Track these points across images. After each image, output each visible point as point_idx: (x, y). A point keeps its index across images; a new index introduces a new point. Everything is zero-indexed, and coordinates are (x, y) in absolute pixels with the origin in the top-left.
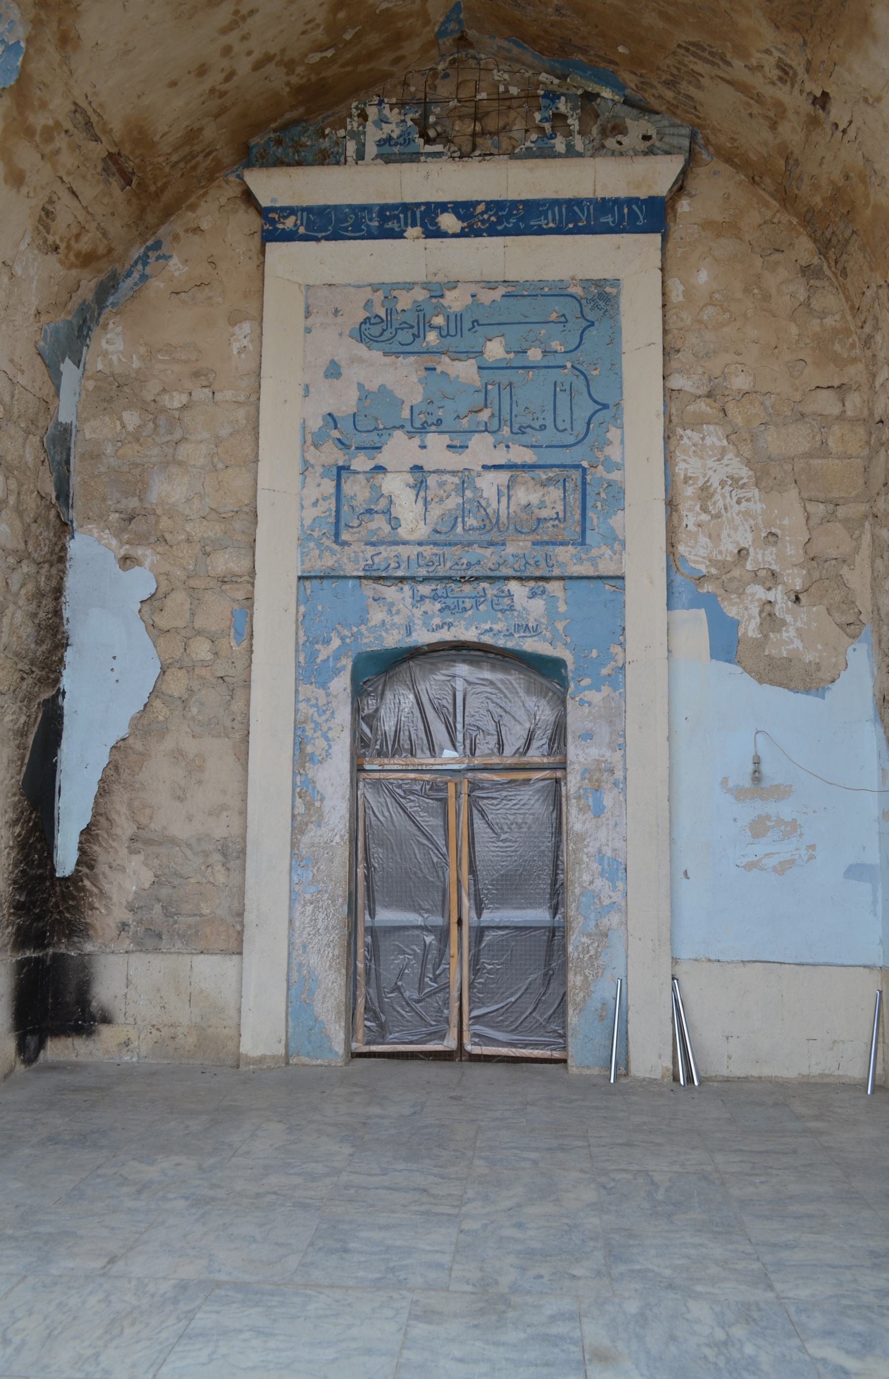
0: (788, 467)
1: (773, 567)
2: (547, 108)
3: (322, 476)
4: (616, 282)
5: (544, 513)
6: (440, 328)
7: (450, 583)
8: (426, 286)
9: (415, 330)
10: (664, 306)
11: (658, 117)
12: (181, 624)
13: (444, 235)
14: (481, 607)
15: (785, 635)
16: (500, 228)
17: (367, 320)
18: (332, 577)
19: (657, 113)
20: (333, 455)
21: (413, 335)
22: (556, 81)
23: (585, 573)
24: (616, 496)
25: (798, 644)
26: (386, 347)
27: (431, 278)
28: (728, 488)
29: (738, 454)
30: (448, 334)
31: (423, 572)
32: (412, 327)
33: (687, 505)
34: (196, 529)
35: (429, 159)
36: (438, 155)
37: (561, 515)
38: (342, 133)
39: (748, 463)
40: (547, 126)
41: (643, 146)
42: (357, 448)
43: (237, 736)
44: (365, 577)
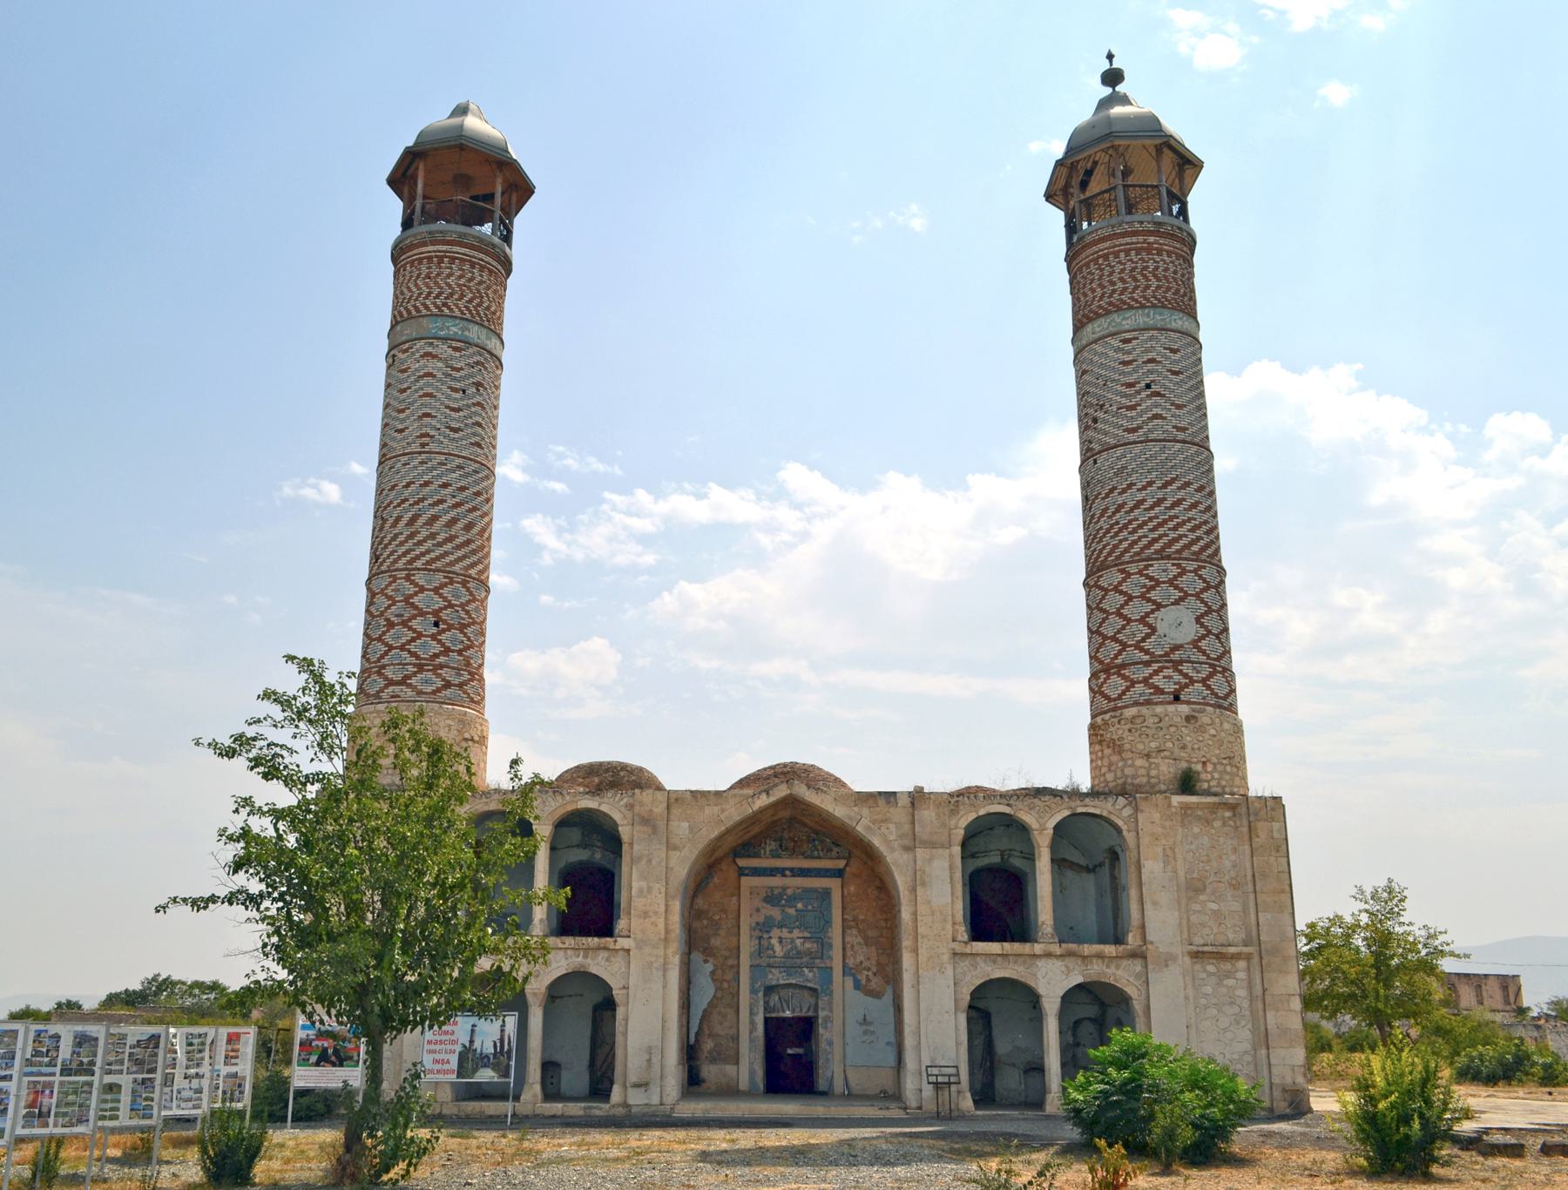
7: (788, 969)
20: (758, 933)
24: (831, 946)
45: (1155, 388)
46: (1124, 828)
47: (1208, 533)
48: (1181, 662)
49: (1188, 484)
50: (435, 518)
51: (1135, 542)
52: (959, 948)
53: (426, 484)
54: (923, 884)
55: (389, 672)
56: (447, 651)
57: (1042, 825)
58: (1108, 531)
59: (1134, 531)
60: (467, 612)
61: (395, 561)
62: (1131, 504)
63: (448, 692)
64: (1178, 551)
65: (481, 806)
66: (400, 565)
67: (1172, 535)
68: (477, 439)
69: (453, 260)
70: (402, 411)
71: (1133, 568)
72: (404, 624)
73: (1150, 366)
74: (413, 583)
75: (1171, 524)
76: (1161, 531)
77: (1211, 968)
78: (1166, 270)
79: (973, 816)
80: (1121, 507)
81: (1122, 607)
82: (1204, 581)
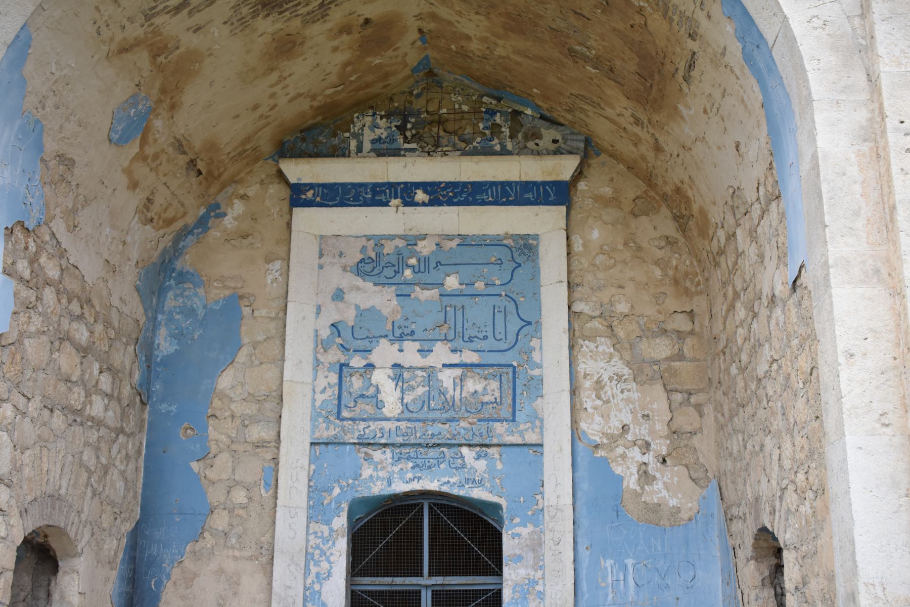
0: (656, 367)
1: (647, 438)
2: (488, 120)
3: (329, 370)
4: (536, 237)
5: (486, 399)
6: (413, 266)
8: (403, 237)
9: (396, 268)
10: (568, 254)
11: (563, 128)
12: (224, 476)
13: (417, 204)
14: (442, 466)
15: (655, 487)
16: (455, 200)
17: (362, 261)
18: (335, 443)
19: (562, 125)
20: (335, 356)
21: (395, 271)
22: (494, 102)
23: (515, 442)
24: (536, 385)
25: (665, 493)
26: (376, 279)
27: (407, 232)
28: (614, 382)
29: (621, 358)
30: (419, 271)
31: (400, 440)
32: (394, 266)
33: (586, 394)
34: (238, 408)
35: (407, 153)
36: (413, 150)
37: (498, 400)
38: (347, 135)
39: (628, 364)
40: (487, 132)
41: (553, 147)
42: (354, 351)
43: (264, 560)
44: (358, 444)
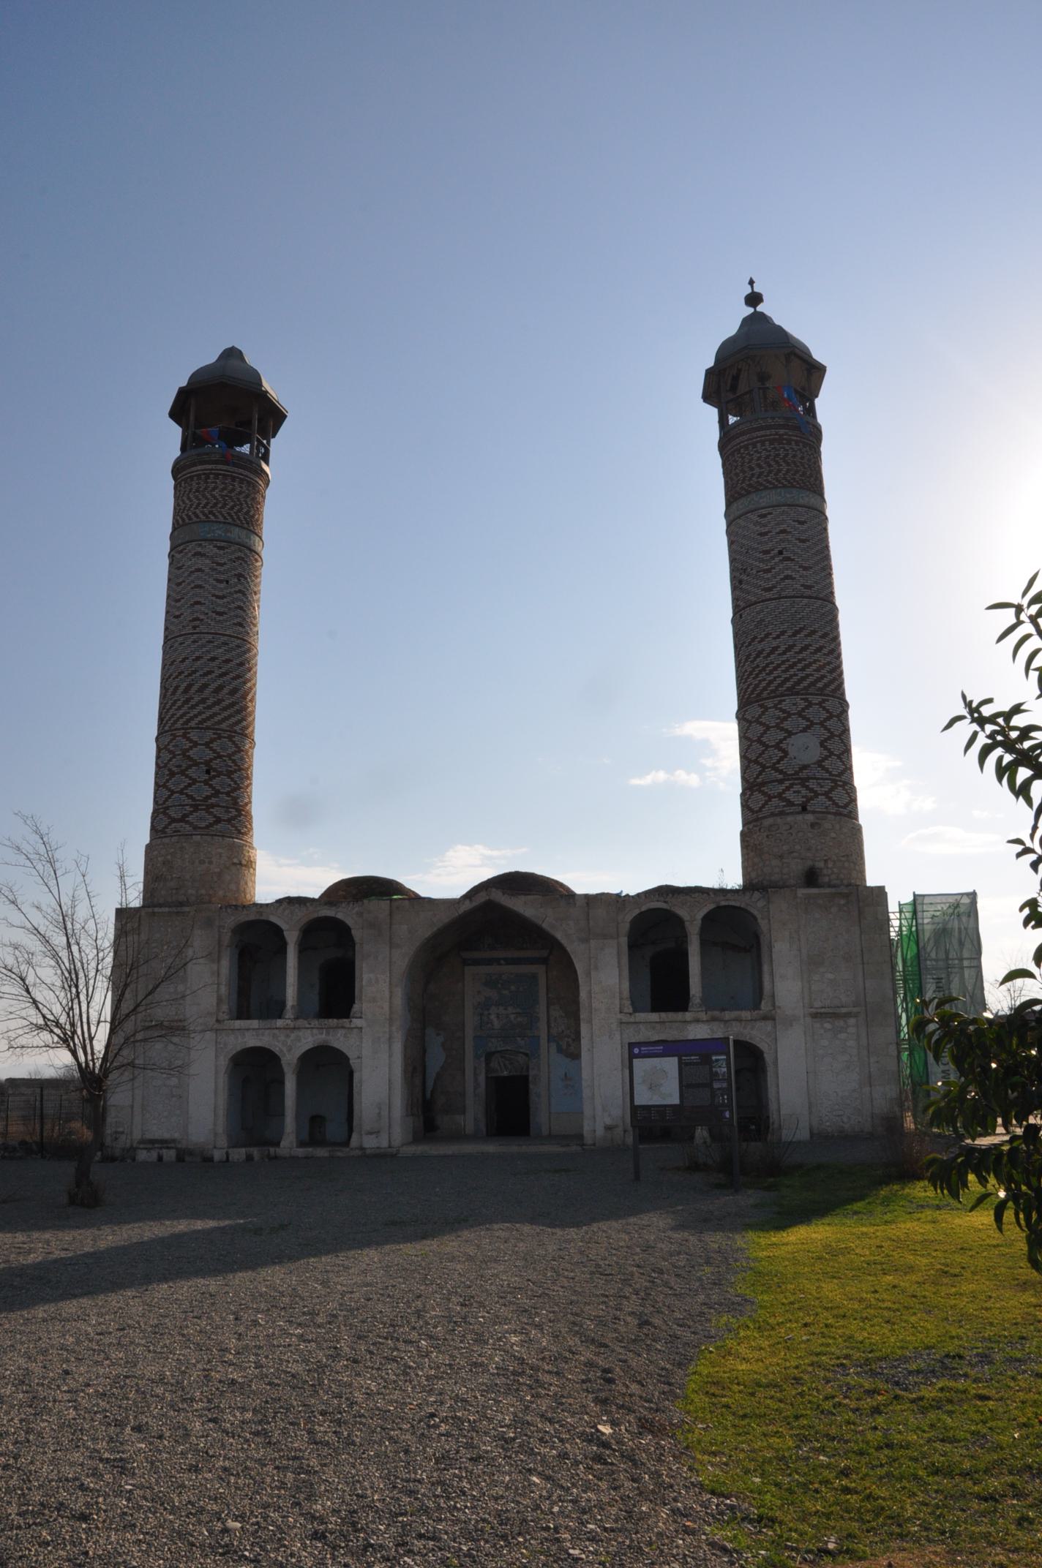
45: (786, 554)
46: (759, 916)
47: (831, 671)
48: (808, 779)
49: (814, 632)
50: (205, 686)
51: (771, 682)
52: (625, 1019)
53: (198, 658)
54: (596, 968)
55: (172, 812)
56: (217, 793)
57: (693, 919)
58: (751, 673)
59: (771, 672)
60: (234, 761)
61: (175, 722)
62: (768, 650)
63: (218, 826)
64: (805, 688)
65: (244, 917)
66: (178, 725)
67: (801, 674)
68: (239, 620)
69: (217, 476)
70: (178, 601)
71: (769, 703)
72: (183, 773)
73: (782, 536)
74: (188, 739)
75: (800, 666)
76: (792, 672)
77: (827, 1026)
78: (794, 456)
79: (637, 912)
80: (760, 652)
81: (762, 735)
82: (828, 711)
